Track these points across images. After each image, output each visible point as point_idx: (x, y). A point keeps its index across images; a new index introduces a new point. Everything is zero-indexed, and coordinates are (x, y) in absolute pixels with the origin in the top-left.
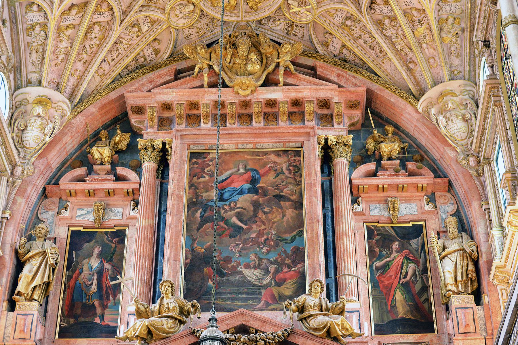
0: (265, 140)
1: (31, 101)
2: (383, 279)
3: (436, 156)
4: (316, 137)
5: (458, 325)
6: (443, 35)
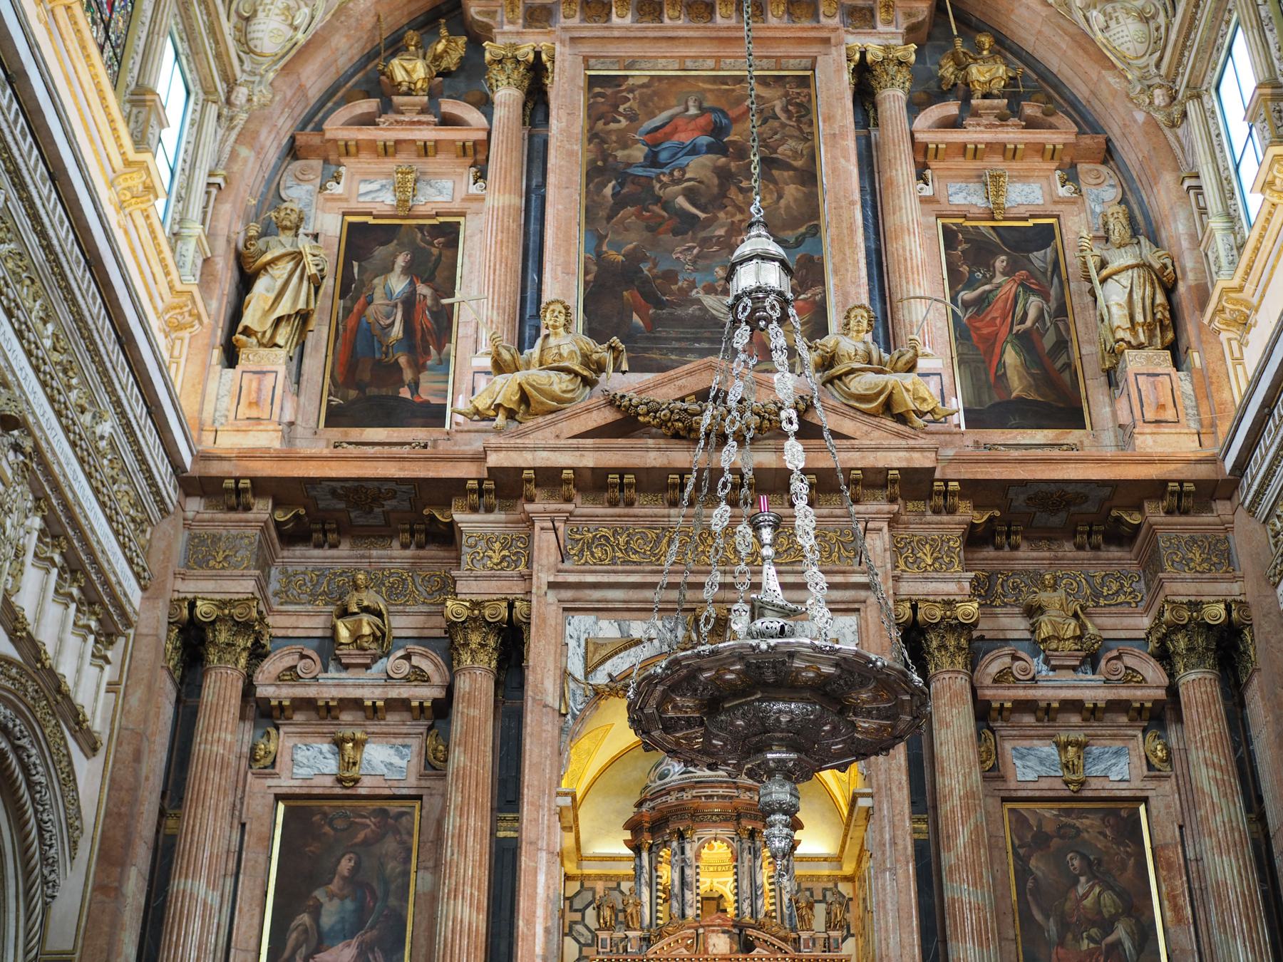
2: (977, 324)
3: (1081, 90)
4: (844, 47)
5: (1142, 406)
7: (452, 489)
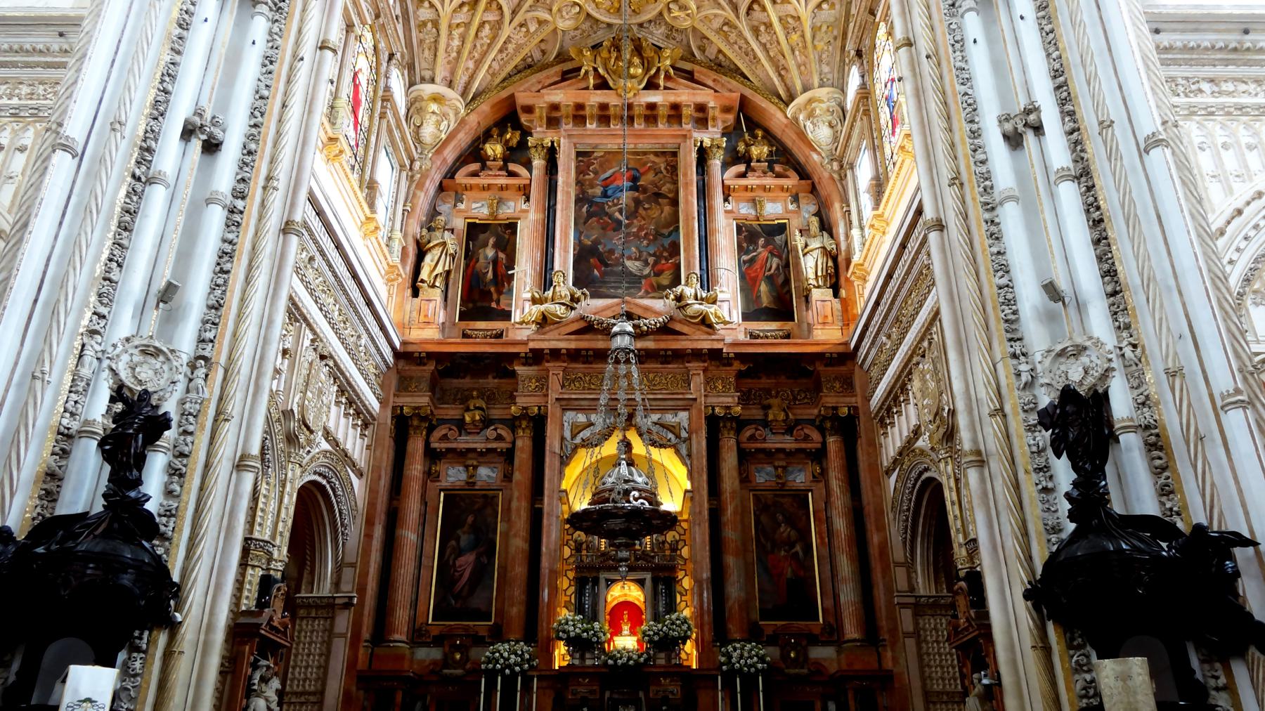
0: (646, 141)
1: (425, 98)
3: (802, 159)
6: (816, 43)
7: (516, 356)
